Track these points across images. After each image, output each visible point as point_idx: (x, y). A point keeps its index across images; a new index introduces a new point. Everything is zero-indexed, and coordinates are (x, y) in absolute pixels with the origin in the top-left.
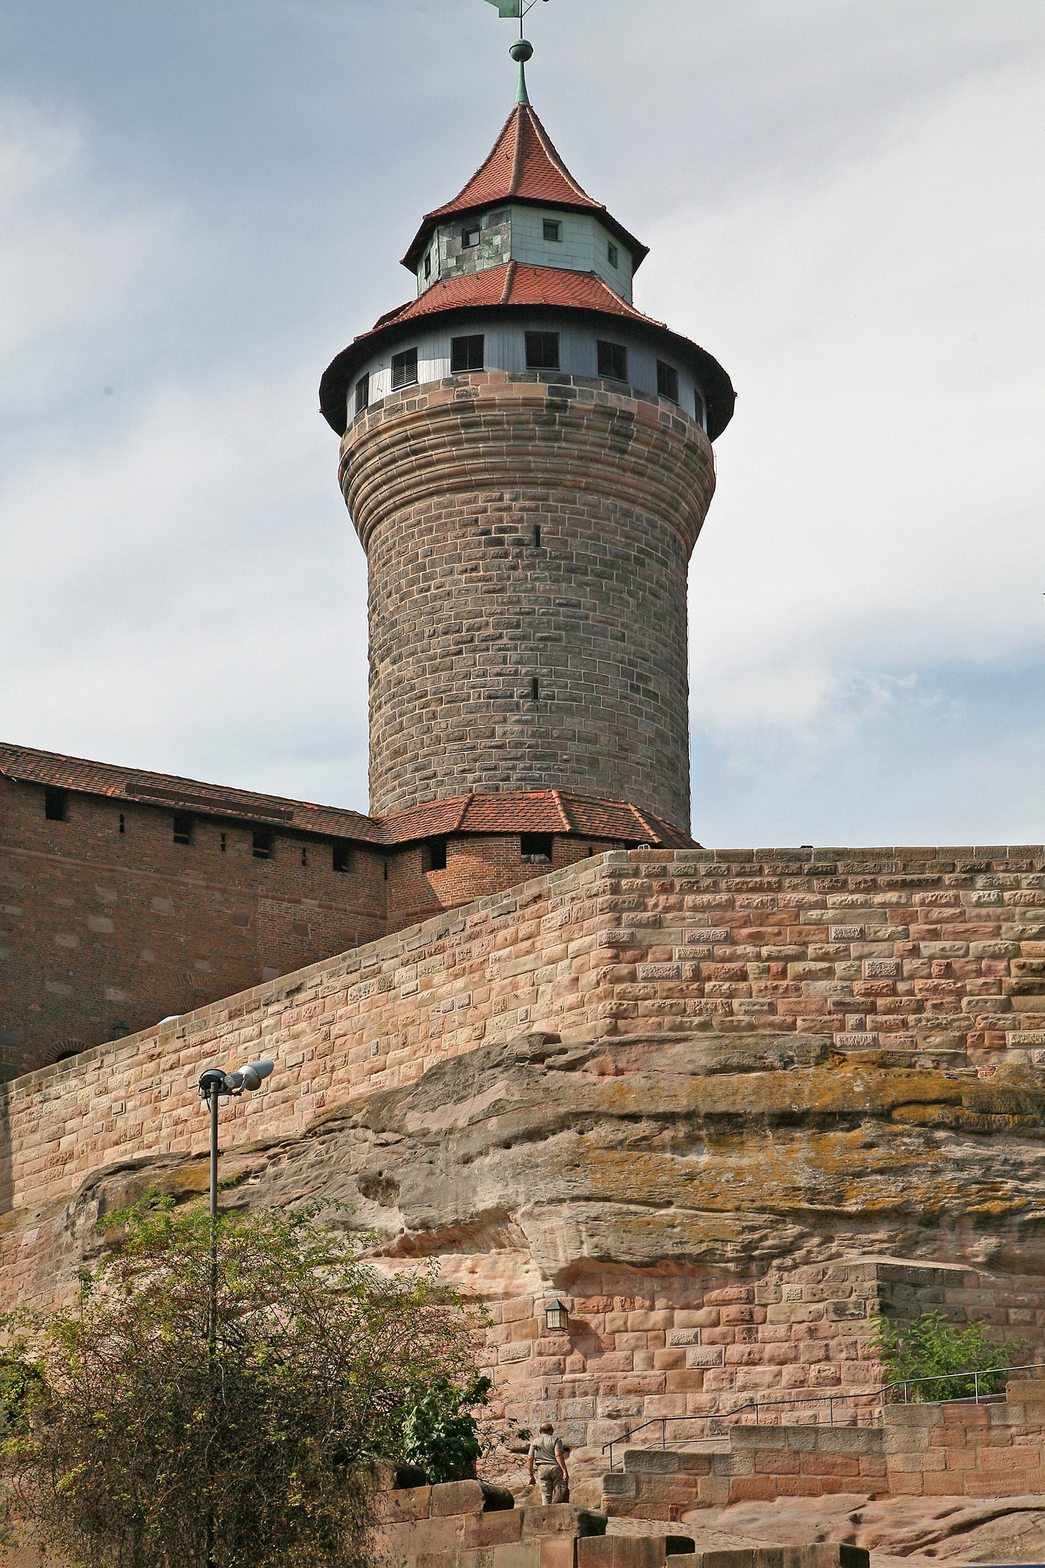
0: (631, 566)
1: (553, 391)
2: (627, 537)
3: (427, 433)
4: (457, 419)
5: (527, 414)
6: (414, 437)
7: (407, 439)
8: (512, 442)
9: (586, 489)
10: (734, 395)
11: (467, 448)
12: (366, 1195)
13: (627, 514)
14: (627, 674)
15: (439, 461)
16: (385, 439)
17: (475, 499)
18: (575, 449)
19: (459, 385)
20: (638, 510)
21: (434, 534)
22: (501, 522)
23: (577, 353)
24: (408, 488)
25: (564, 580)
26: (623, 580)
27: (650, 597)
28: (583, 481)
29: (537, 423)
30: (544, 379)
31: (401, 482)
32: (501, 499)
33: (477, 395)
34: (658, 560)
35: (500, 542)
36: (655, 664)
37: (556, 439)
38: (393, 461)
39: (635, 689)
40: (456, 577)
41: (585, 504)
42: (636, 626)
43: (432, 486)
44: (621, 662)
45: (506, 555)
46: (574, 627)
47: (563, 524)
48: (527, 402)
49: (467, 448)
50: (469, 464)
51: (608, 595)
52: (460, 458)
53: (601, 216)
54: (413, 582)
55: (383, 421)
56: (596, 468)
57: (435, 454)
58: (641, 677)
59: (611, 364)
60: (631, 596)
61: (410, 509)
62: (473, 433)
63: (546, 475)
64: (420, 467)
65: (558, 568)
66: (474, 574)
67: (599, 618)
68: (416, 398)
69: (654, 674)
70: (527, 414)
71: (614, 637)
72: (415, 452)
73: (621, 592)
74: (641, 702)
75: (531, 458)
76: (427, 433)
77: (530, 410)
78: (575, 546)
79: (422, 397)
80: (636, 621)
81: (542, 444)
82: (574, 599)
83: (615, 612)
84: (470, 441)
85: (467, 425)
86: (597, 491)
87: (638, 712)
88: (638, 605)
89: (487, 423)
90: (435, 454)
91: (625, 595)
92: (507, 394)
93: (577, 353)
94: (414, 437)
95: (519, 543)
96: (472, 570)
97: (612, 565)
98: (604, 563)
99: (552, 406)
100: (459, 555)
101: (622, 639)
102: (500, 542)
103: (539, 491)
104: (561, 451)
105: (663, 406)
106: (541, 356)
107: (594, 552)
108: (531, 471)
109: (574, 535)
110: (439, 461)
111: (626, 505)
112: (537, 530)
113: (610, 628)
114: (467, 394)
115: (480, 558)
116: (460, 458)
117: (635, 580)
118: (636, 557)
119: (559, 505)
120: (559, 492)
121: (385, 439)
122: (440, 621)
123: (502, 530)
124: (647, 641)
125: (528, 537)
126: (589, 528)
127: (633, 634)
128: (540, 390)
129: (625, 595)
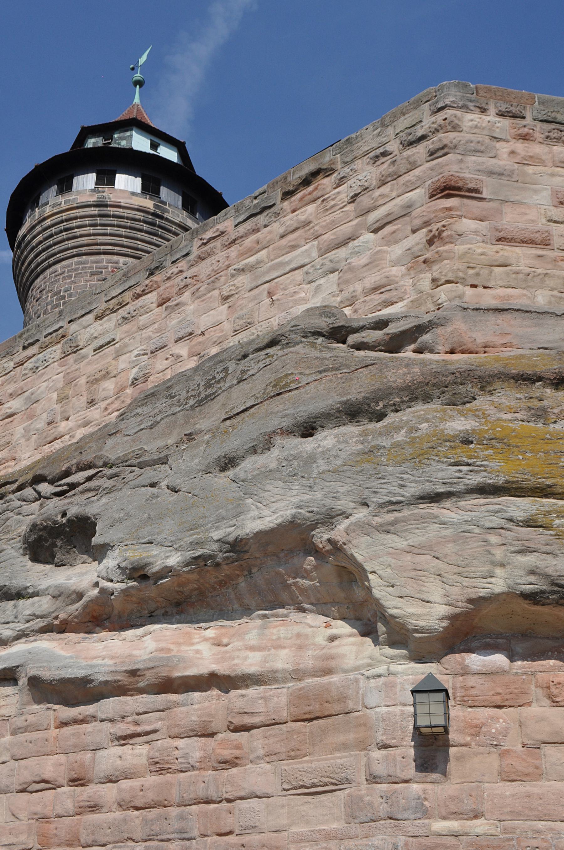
3: (76, 218)
6: (67, 220)
7: (62, 222)
8: (128, 230)
11: (99, 230)
12: (35, 559)
15: (81, 236)
16: (48, 222)
17: (101, 261)
19: (99, 192)
21: (73, 279)
24: (59, 252)
31: (56, 248)
38: (51, 236)
43: (75, 251)
49: (99, 230)
50: (100, 239)
52: (94, 235)
55: (48, 210)
57: (78, 232)
61: (58, 266)
64: (68, 239)
68: (71, 198)
72: (66, 230)
76: (76, 218)
77: (142, 214)
79: (73, 197)
84: (102, 225)
89: (114, 216)
92: (129, 201)
94: (67, 220)
110: (81, 236)
116: (94, 235)
121: (48, 222)
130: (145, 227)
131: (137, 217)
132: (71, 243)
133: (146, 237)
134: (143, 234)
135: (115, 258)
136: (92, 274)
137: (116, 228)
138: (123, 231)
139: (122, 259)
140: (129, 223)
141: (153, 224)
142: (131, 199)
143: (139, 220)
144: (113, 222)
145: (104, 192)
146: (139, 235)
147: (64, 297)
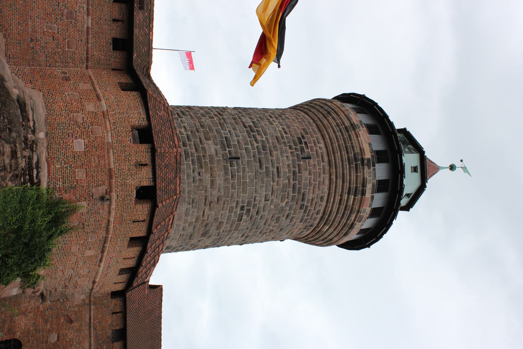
0: (300, 203)
1: (368, 160)
2: (312, 200)
4: (347, 124)
5: (357, 150)
8: (344, 145)
9: (330, 179)
13: (322, 198)
14: (249, 203)
15: (328, 120)
18: (347, 171)
20: (324, 204)
22: (309, 143)
23: (381, 171)
25: (289, 170)
27: (287, 214)
28: (334, 177)
29: (355, 154)
30: (372, 156)
32: (319, 143)
33: (360, 130)
35: (301, 142)
36: (256, 218)
39: (242, 208)
40: (280, 127)
41: (324, 178)
42: (272, 207)
44: (255, 200)
45: (295, 144)
47: (314, 169)
48: (362, 150)
51: (286, 192)
56: (340, 182)
58: (249, 211)
60: (286, 203)
63: (333, 161)
65: (294, 167)
66: (283, 133)
67: (274, 187)
69: (251, 218)
70: (357, 150)
71: (266, 196)
73: (288, 198)
74: (236, 212)
75: (339, 154)
77: (359, 151)
78: (305, 174)
80: (275, 206)
81: (346, 157)
82: (282, 174)
83: (278, 195)
84: (340, 129)
85: (346, 128)
86: (330, 184)
87: (230, 211)
88: (283, 208)
89: (349, 135)
90: (330, 118)
91: (286, 200)
93: (381, 171)
95: (302, 150)
96: (285, 132)
97: (299, 193)
98: (300, 189)
99: (363, 160)
100: (290, 128)
101: (266, 200)
102: (301, 142)
103: (326, 159)
104: (345, 165)
105: (368, 210)
107: (304, 184)
108: (334, 154)
109: (310, 174)
110: (328, 120)
111: (325, 198)
112: (309, 158)
113: (270, 193)
114: (359, 128)
115: (291, 135)
116: (332, 127)
117: (293, 205)
118: (304, 204)
119: (322, 167)
120: (327, 168)
122: (258, 120)
123: (306, 143)
125: (306, 155)
126: (314, 180)
127: (269, 205)
128: (368, 155)
129: (286, 200)
130: (352, 155)
131: (355, 149)
133: (345, 157)
134: (346, 155)
137: (342, 138)
138: (342, 142)
139: (322, 145)
140: (349, 144)
141: (356, 160)
142: (366, 143)
143: (354, 150)
144: (345, 135)
145: (363, 127)
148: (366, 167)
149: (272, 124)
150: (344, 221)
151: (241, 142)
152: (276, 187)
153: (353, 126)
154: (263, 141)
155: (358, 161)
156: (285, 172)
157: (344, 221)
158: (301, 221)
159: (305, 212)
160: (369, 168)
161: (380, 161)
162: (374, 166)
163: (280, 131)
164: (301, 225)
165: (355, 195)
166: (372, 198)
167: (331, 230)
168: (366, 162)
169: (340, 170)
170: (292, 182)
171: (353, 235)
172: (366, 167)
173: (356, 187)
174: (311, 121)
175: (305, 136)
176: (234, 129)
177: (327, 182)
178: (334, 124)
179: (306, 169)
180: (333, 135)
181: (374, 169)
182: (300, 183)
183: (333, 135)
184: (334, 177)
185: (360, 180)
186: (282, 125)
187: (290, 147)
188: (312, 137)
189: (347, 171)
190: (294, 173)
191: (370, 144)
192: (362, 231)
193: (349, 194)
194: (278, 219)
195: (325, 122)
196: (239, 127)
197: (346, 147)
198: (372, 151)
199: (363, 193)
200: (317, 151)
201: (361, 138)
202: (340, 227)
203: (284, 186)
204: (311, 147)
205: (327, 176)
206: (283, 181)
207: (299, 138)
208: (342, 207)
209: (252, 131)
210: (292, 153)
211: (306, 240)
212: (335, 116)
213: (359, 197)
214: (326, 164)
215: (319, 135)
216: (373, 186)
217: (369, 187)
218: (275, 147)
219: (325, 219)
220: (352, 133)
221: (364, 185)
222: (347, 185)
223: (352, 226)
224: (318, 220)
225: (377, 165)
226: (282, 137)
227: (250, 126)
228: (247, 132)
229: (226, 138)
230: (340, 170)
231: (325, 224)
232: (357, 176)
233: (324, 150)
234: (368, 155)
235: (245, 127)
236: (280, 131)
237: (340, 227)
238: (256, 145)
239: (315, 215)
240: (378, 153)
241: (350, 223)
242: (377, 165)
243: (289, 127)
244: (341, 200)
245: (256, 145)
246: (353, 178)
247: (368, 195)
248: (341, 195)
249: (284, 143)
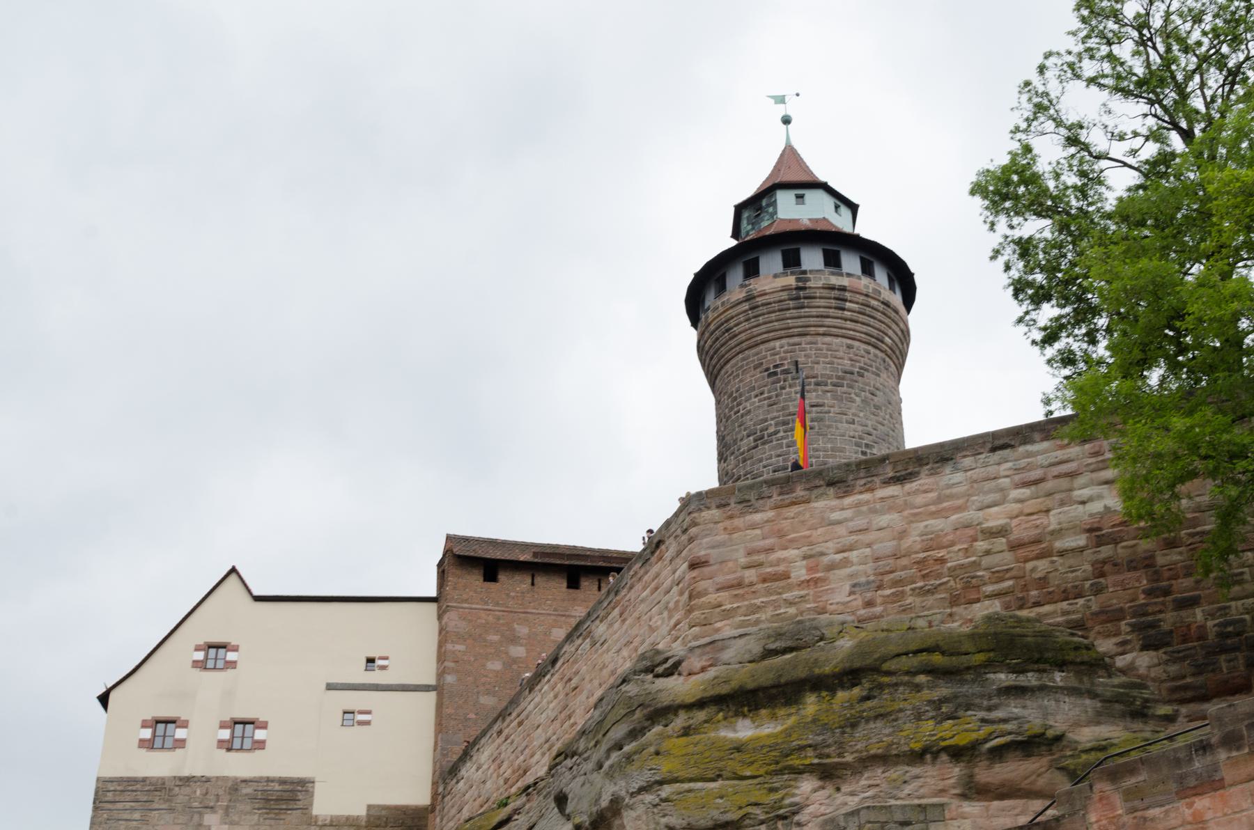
0: (855, 377)
1: (798, 280)
4: (746, 306)
5: (784, 295)
6: (726, 321)
9: (824, 335)
10: (912, 275)
11: (753, 322)
13: (850, 347)
14: (858, 445)
18: (814, 311)
20: (856, 344)
23: (812, 259)
26: (850, 386)
28: (821, 330)
30: (792, 273)
34: (873, 373)
35: (775, 374)
37: (803, 307)
42: (861, 414)
46: (821, 420)
48: (785, 289)
53: (825, 187)
54: (732, 408)
56: (828, 321)
59: (832, 261)
62: (757, 312)
70: (784, 295)
71: (848, 422)
77: (785, 293)
78: (819, 369)
89: (763, 305)
93: (812, 259)
95: (786, 372)
97: (843, 378)
98: (838, 377)
99: (799, 288)
101: (853, 423)
102: (775, 374)
103: (796, 340)
105: (865, 281)
106: (792, 261)
111: (849, 342)
120: (809, 338)
124: (870, 423)
125: (793, 368)
128: (791, 280)
132: (733, 343)
133: (794, 312)
135: (772, 344)
136: (755, 368)
139: (777, 344)
141: (798, 298)
146: (788, 314)
147: (735, 399)
148: (808, 284)
149: (749, 412)
150: (878, 315)
151: (779, 452)
152: (837, 409)
153: (749, 298)
154: (776, 425)
155: (800, 295)
156: (817, 397)
157: (878, 315)
158: (878, 375)
159: (867, 370)
160: (808, 280)
161: (797, 263)
162: (805, 272)
163: (760, 401)
164: (884, 375)
165: (846, 300)
166: (849, 275)
167: (890, 333)
168: (800, 284)
169: (813, 321)
170: (829, 388)
171: (896, 299)
172: (808, 284)
173: (835, 298)
174: (740, 356)
175: (764, 366)
176: (761, 460)
177: (828, 339)
178: (746, 325)
179: (812, 368)
180: (763, 328)
181: (811, 271)
182: (830, 377)
183: (763, 328)
184: (821, 330)
185: (825, 293)
186: (750, 398)
187: (783, 388)
188: (765, 357)
189: (814, 311)
190: (817, 384)
191: (776, 276)
192: (892, 288)
193: (843, 309)
194: (877, 407)
195: (743, 336)
196: (757, 454)
197: (780, 310)
198: (785, 274)
199: (843, 289)
200: (786, 352)
201: (767, 288)
202: (887, 320)
203: (835, 397)
204: (782, 359)
205: (819, 339)
206: (828, 399)
207: (770, 375)
208: (862, 318)
209: (762, 437)
210: (790, 386)
211: (900, 367)
212: (732, 323)
213: (848, 295)
214: (803, 339)
215: (762, 347)
216: (833, 274)
217: (835, 281)
218: (783, 408)
219: (875, 342)
220: (760, 300)
221: (832, 288)
222: (832, 312)
223: (886, 304)
224: (877, 352)
225: (804, 267)
226: (769, 398)
227: (755, 440)
228: (764, 444)
229: (774, 471)
230: (813, 321)
231: (882, 342)
232: (821, 298)
233: (784, 341)
234: (791, 280)
235: (756, 447)
236: (760, 401)
237: (887, 320)
238: (781, 434)
239: (871, 356)
240: (787, 264)
241: (881, 307)
242: (804, 267)
243: (753, 389)
244: (852, 321)
245: (781, 434)
246: (822, 302)
247: (845, 282)
248: (846, 320)
249: (777, 396)
